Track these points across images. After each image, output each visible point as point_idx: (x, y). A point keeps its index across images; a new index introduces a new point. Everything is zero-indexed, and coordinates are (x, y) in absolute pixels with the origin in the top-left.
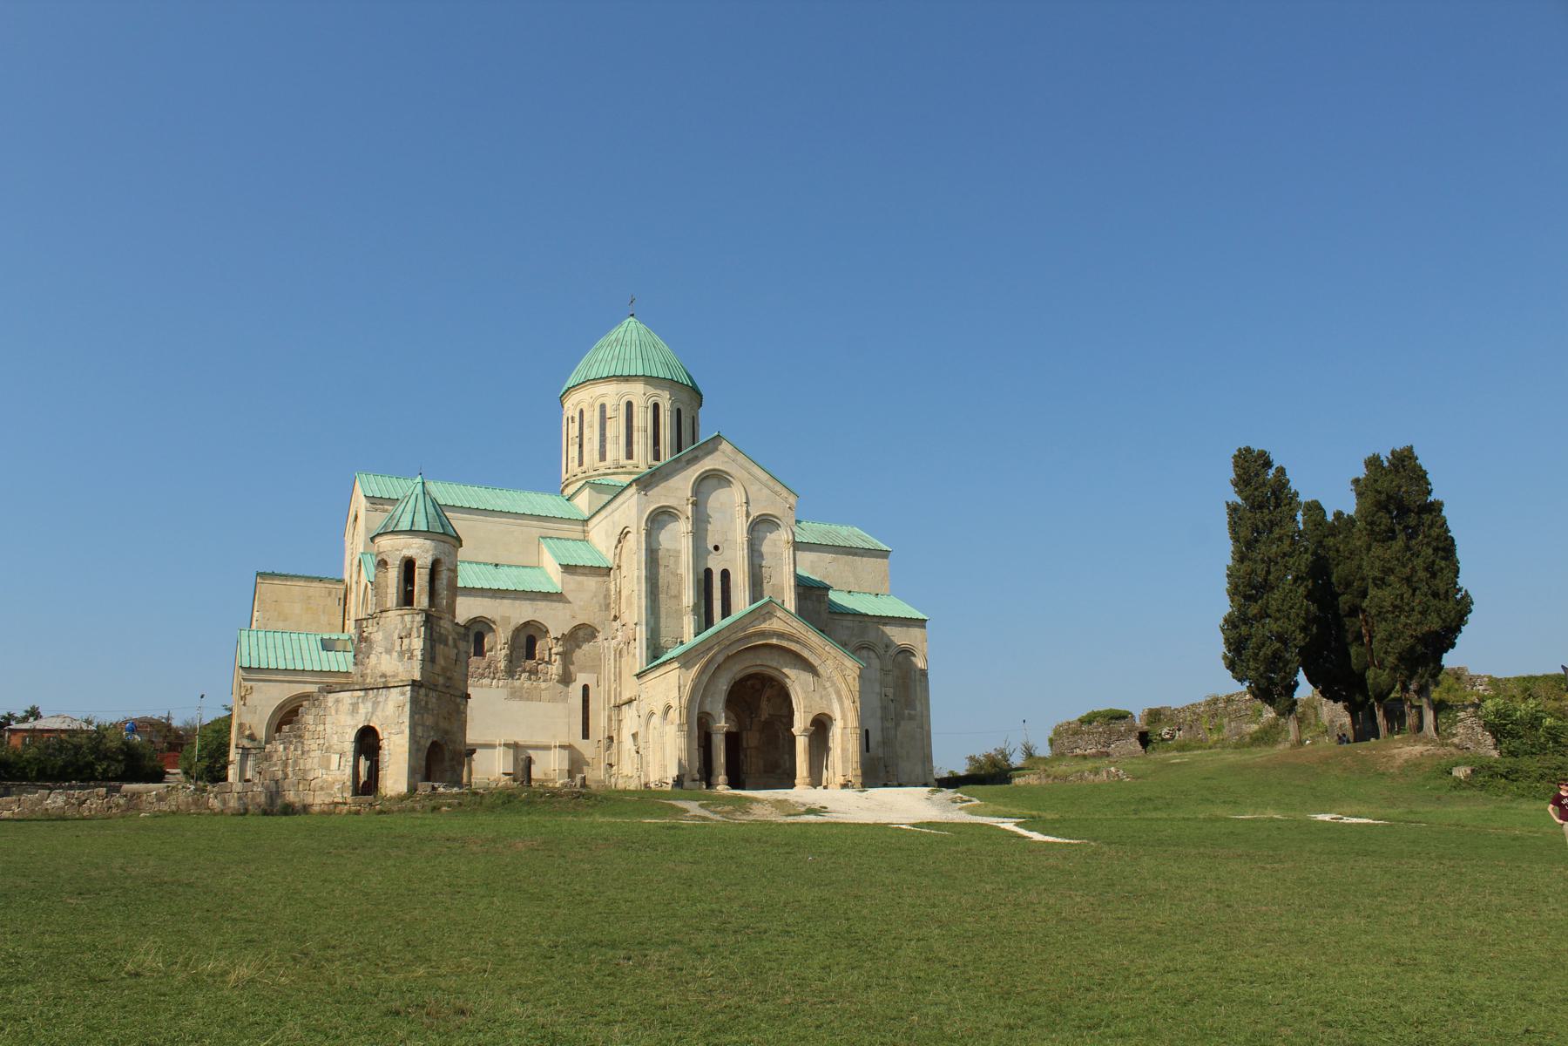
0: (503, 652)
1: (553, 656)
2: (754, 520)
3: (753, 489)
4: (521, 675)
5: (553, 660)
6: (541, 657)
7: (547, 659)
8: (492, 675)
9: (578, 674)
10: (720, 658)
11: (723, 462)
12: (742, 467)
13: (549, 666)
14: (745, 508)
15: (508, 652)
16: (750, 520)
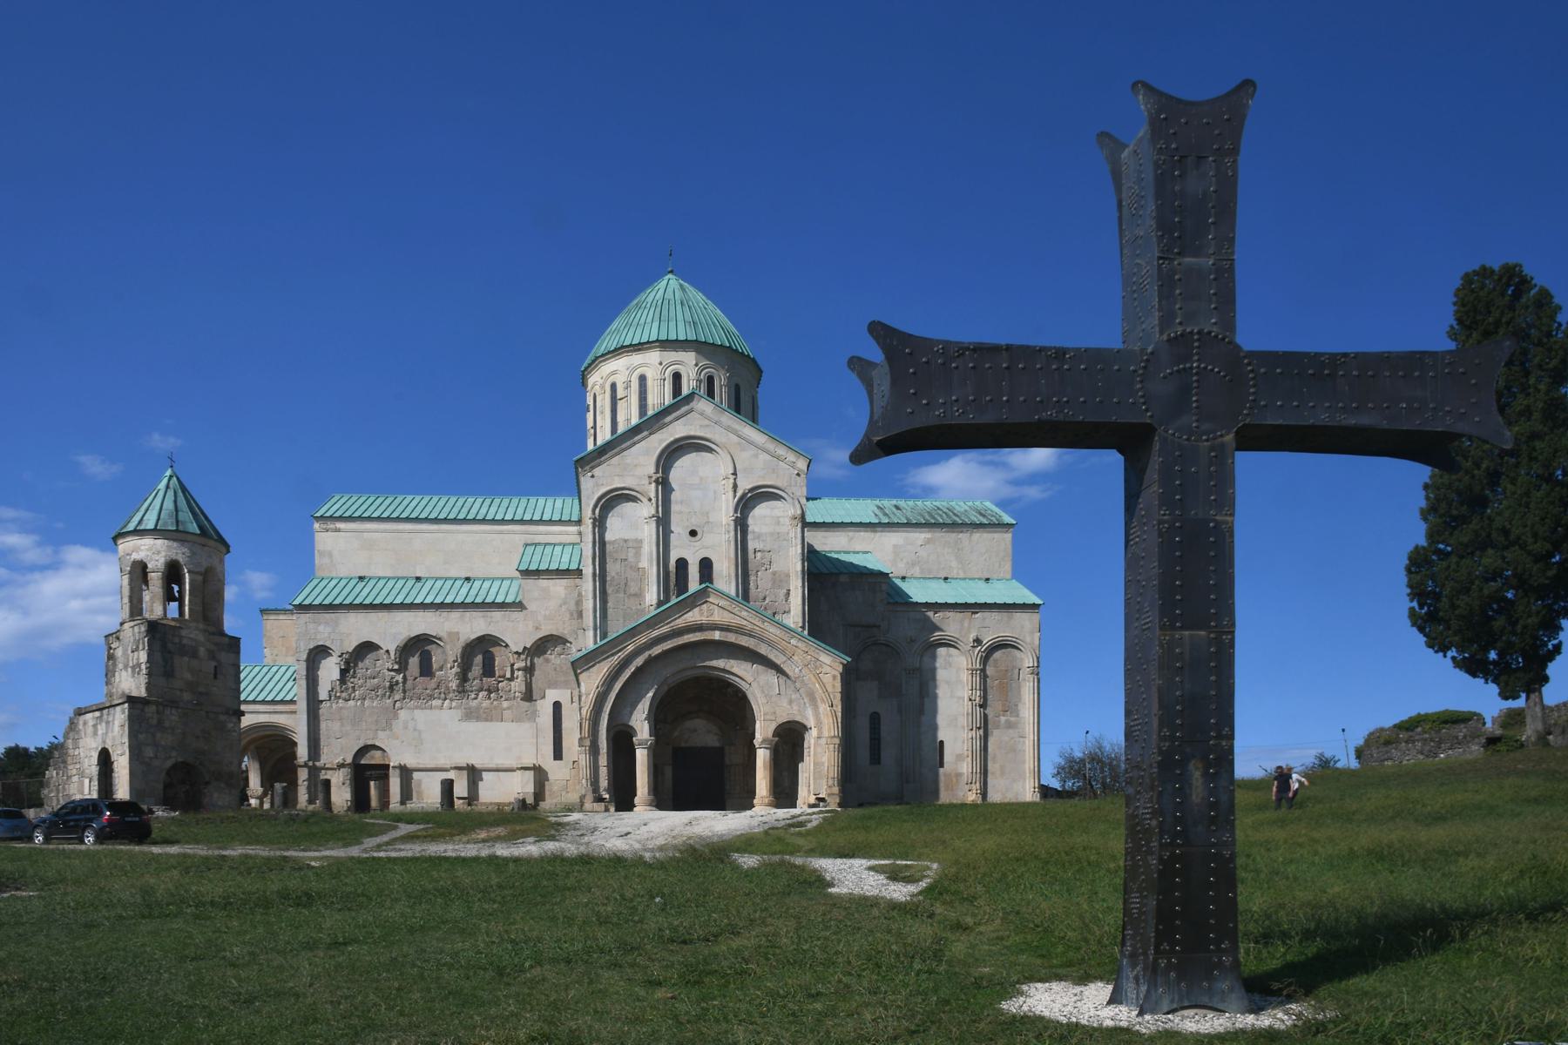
0: (456, 669)
1: (516, 673)
2: (744, 495)
3: (744, 457)
4: (477, 695)
5: (515, 676)
6: (502, 673)
7: (508, 675)
8: (443, 695)
9: (547, 691)
10: (639, 661)
11: (701, 426)
12: (728, 429)
13: (513, 683)
14: (732, 481)
15: (459, 670)
16: (739, 494)
